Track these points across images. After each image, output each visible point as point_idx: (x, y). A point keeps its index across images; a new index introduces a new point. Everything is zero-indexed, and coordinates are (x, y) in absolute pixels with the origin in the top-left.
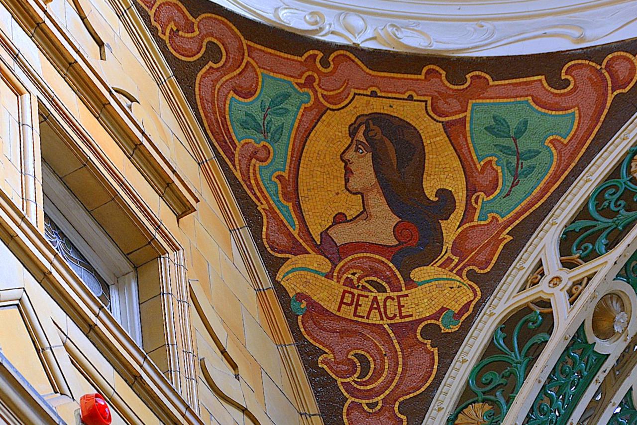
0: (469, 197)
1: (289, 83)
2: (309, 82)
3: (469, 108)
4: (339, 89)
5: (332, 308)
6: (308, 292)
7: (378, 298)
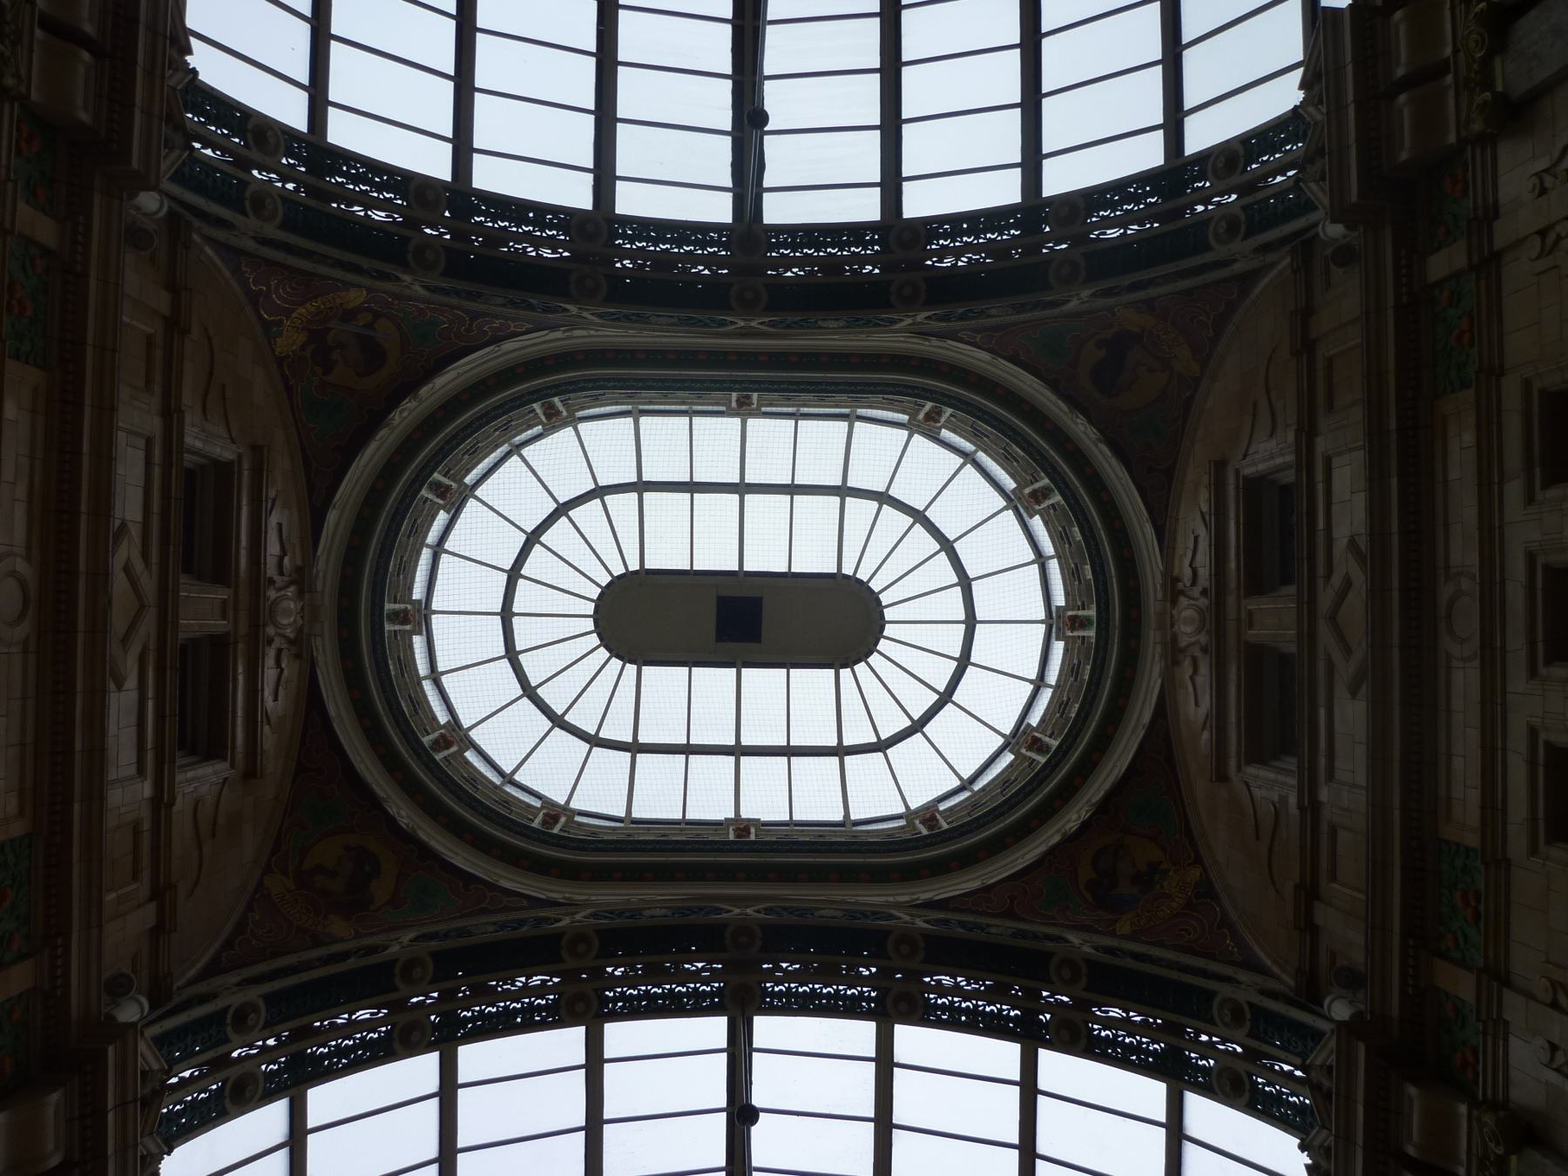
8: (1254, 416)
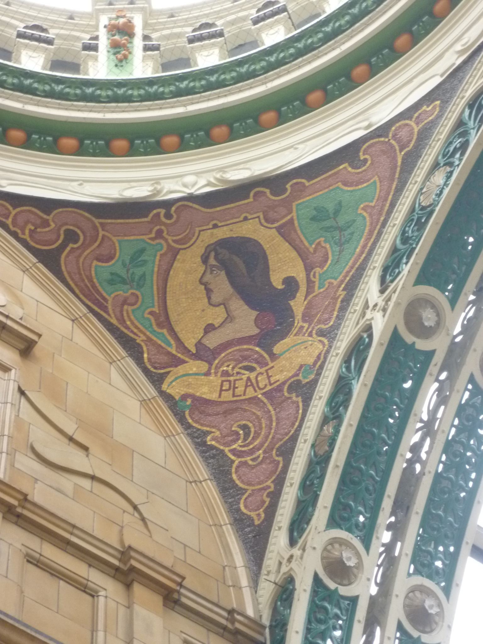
0: (308, 276)
1: (143, 240)
2: (159, 234)
3: (294, 209)
4: (185, 232)
5: (214, 396)
6: (191, 391)
7: (251, 377)
8: (71, 439)
